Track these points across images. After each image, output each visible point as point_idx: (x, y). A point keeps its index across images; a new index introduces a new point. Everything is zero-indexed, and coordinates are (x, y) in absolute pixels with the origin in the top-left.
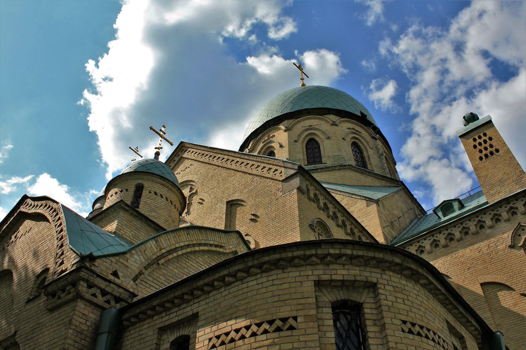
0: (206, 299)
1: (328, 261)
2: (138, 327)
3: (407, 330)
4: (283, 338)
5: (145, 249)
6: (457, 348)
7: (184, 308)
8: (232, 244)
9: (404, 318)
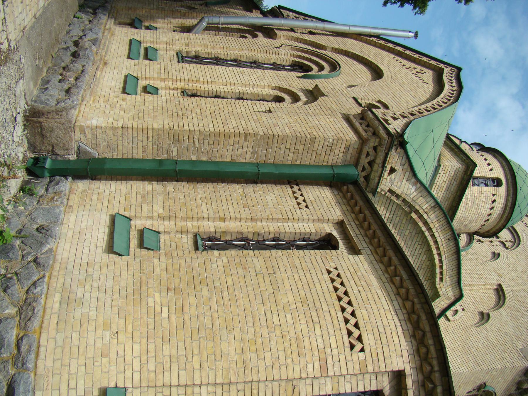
1: (428, 386)
4: (341, 339)
7: (365, 240)
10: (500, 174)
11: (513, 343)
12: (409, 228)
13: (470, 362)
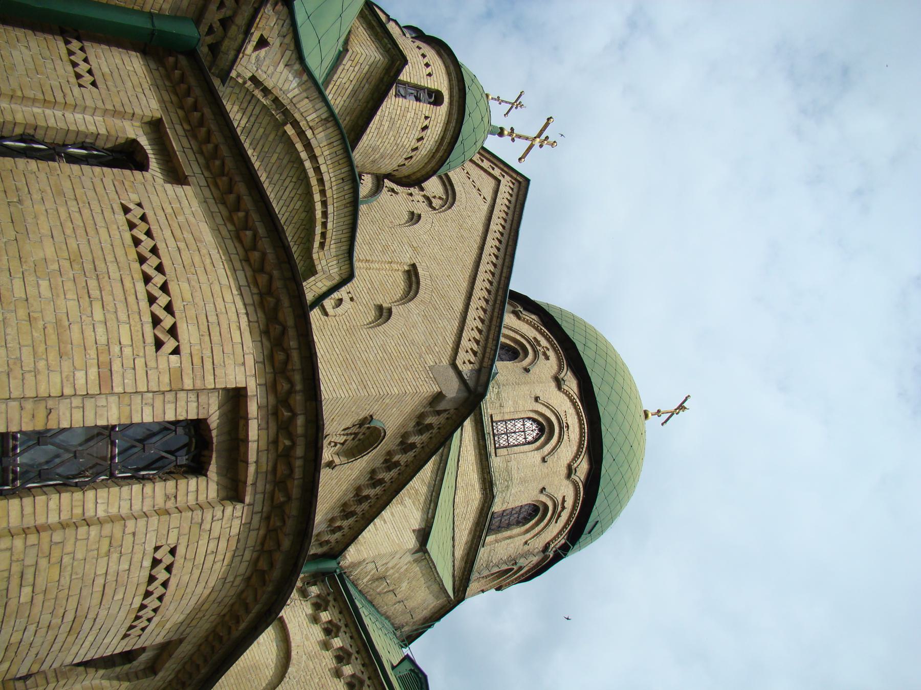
0: (214, 198)
1: (283, 414)
2: (164, 83)
3: (158, 555)
4: (140, 330)
5: (310, 99)
6: (135, 660)
7: (197, 161)
8: (329, 265)
9: (180, 551)
10: (442, 85)
11: (421, 356)
12: (278, 150)
13: (353, 383)
